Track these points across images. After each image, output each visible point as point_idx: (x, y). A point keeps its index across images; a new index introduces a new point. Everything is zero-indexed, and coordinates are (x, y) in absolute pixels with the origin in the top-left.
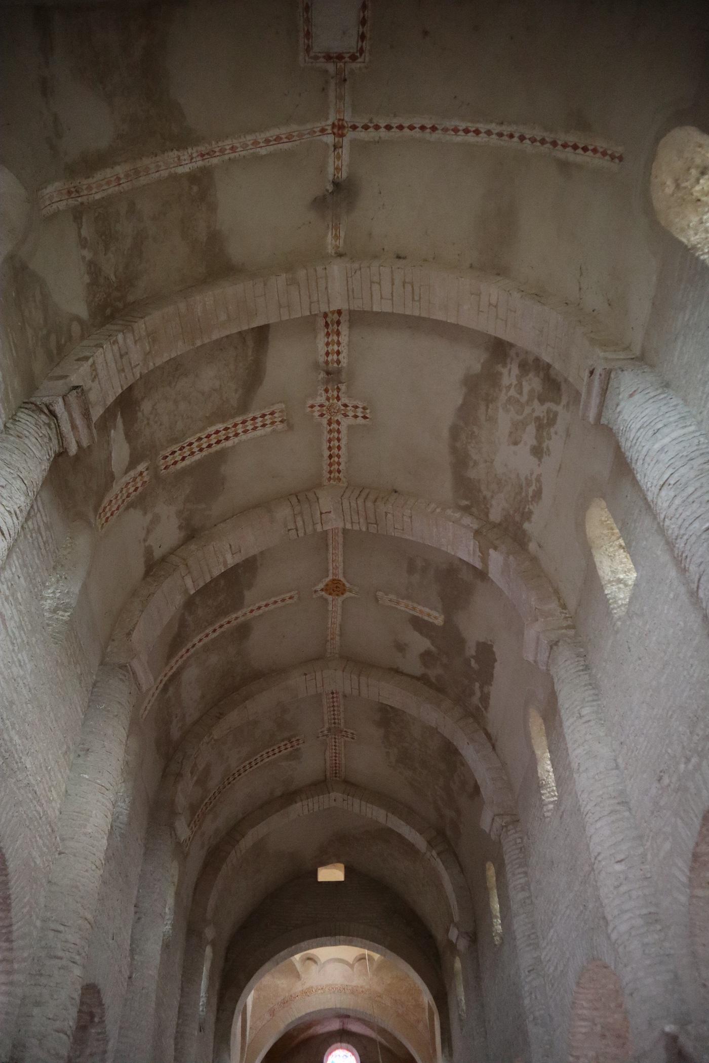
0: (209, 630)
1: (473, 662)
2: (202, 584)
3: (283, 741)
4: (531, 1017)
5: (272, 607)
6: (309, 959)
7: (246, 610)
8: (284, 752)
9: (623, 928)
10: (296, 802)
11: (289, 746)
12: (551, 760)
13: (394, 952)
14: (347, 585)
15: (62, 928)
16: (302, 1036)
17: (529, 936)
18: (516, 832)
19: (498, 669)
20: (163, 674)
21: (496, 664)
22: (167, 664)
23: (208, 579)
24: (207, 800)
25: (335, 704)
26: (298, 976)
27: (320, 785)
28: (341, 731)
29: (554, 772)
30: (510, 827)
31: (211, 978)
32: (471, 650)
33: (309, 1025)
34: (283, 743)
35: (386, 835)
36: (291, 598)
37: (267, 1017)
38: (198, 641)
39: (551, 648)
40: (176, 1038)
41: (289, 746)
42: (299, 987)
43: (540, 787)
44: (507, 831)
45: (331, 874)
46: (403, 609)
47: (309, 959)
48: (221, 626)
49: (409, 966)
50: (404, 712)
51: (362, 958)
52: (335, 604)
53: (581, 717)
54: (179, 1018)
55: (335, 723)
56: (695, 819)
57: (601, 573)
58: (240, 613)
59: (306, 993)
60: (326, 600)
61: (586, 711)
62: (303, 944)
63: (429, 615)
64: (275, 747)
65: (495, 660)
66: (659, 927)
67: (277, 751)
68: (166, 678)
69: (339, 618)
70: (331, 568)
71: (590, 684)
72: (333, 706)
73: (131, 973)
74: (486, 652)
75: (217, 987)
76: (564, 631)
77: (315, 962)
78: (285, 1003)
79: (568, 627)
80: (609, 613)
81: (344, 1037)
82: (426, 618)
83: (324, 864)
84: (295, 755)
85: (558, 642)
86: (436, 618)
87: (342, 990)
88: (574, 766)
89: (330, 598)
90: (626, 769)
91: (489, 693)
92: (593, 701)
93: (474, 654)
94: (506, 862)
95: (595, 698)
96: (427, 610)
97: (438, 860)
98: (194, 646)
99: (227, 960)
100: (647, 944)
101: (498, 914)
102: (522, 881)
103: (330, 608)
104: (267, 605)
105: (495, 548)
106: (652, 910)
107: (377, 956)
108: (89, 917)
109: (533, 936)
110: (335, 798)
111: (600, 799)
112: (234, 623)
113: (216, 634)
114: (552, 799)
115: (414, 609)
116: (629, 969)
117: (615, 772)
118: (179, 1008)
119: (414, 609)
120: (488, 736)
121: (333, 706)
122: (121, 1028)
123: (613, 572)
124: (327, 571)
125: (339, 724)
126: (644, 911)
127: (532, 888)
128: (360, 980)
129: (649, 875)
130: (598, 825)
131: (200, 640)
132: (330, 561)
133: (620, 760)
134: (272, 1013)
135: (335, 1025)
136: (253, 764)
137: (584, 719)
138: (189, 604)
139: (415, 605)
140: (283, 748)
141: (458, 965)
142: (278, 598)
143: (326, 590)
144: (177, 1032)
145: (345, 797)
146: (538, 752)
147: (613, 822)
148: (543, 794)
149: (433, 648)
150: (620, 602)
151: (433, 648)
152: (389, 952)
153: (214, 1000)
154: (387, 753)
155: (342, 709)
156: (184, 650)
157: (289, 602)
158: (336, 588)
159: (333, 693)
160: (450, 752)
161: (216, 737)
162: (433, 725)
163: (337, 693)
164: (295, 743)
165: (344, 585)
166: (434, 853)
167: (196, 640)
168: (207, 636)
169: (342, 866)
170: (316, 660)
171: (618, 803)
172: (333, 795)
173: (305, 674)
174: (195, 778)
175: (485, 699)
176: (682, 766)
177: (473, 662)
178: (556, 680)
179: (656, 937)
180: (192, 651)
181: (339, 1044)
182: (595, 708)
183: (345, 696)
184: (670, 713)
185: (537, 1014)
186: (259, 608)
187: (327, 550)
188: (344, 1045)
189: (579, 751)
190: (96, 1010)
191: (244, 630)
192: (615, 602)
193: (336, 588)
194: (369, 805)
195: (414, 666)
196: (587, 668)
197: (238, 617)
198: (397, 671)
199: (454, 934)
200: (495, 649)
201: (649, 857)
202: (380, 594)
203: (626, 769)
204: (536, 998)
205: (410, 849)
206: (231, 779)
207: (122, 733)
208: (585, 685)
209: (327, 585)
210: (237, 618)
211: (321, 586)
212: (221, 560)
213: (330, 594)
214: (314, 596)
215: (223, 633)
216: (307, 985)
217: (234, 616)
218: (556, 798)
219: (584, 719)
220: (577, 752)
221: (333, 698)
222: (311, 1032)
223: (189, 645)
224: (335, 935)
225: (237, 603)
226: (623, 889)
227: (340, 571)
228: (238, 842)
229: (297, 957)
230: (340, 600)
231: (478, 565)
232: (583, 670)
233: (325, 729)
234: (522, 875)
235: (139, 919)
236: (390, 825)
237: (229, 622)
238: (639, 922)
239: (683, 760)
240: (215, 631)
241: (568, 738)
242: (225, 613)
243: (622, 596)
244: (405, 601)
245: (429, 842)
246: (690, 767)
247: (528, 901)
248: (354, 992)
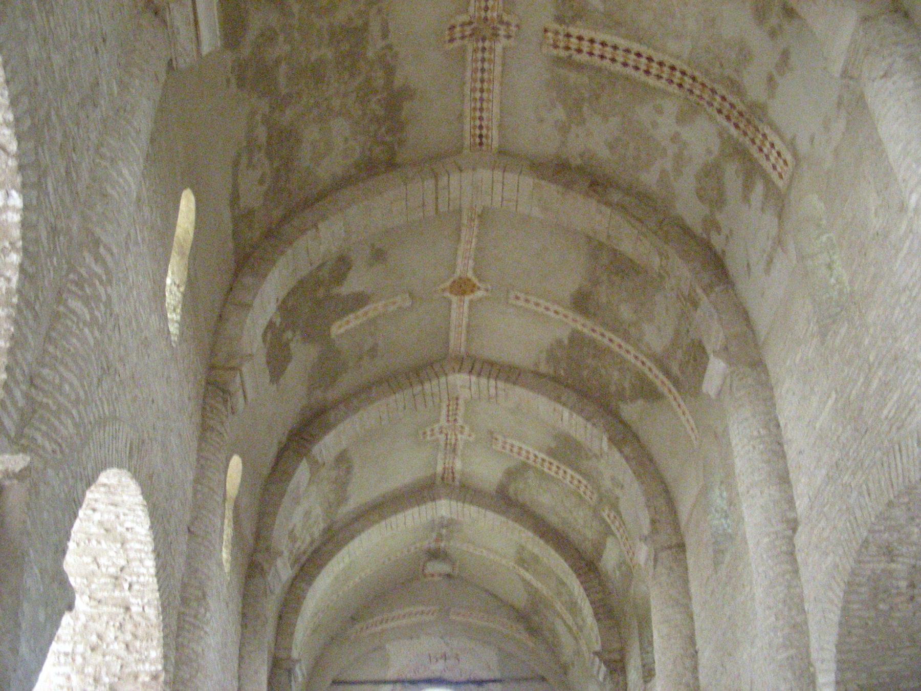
36: (517, 298)
52: (464, 268)
60: (475, 272)
69: (460, 253)
89: (470, 274)
121: (482, 91)
124: (470, 308)
125: (475, 51)
142: (531, 306)
143: (474, 285)
187: (468, 325)
209: (472, 291)
211: (479, 294)
213: (469, 280)
227: (454, 306)
230: (458, 273)
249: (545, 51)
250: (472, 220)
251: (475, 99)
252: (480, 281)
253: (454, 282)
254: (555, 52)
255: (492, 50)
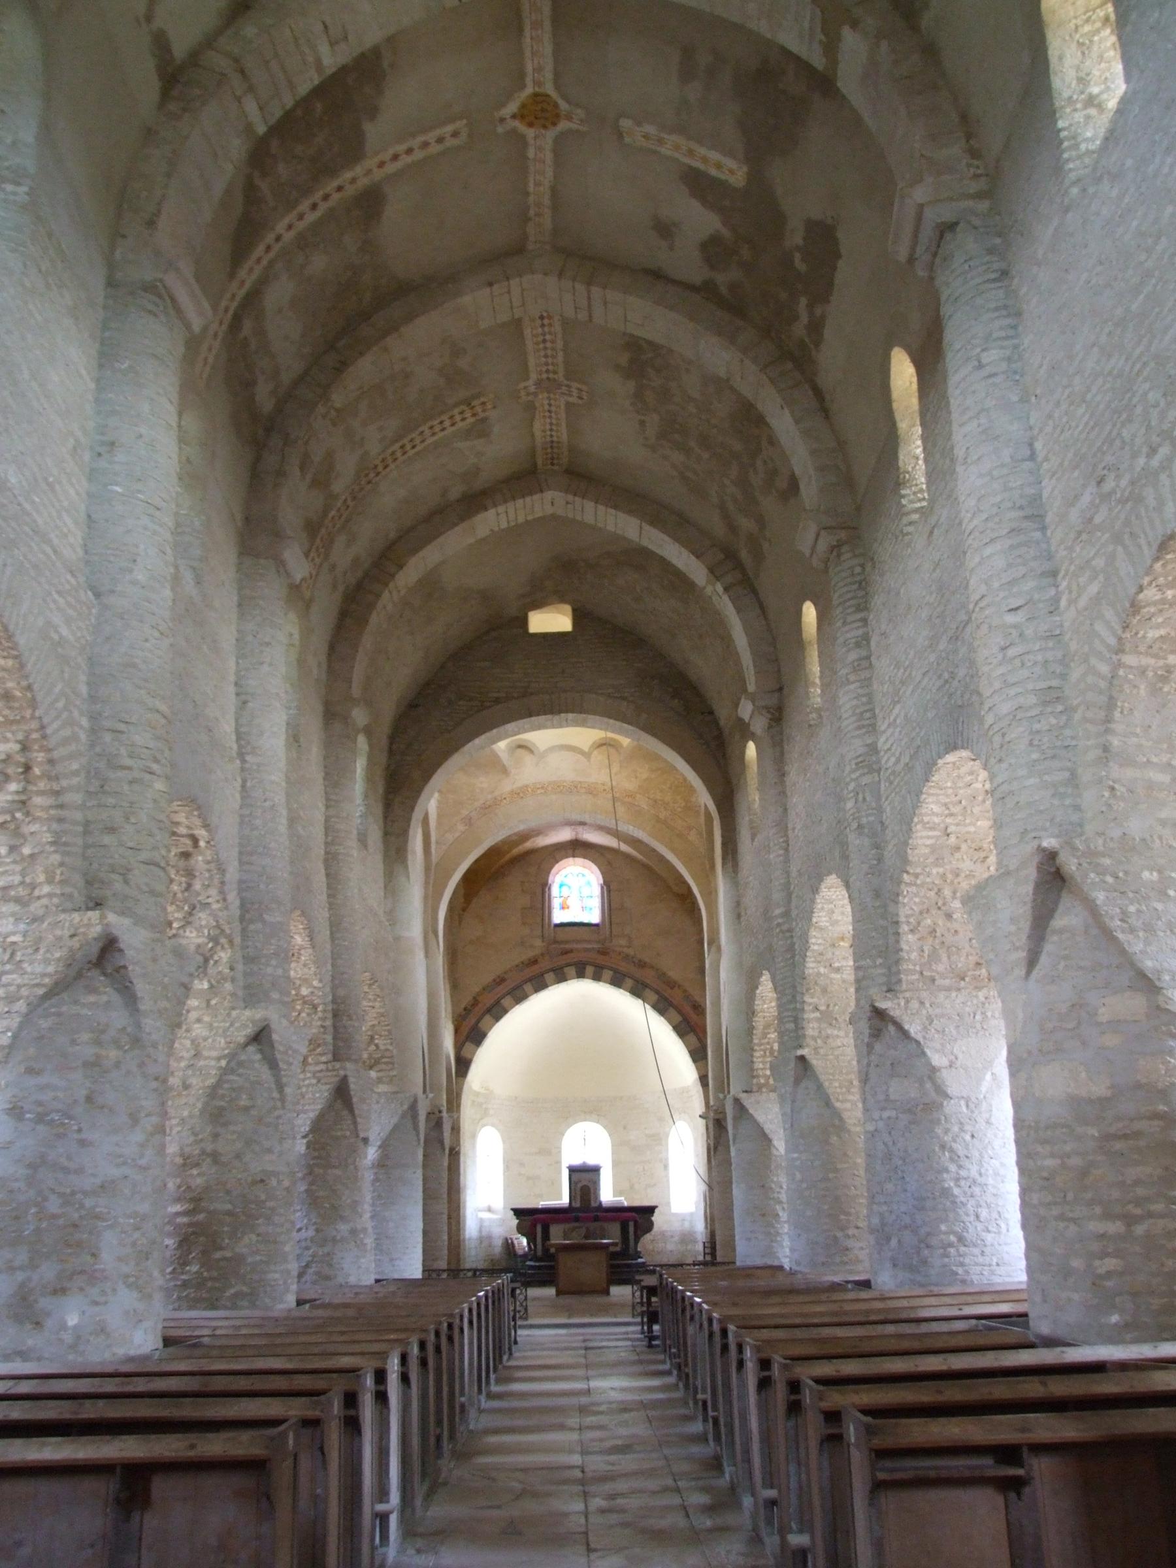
0: (304, 206)
1: (797, 257)
2: (278, 113)
3: (456, 405)
4: (855, 825)
5: (418, 155)
6: (520, 746)
7: (370, 163)
8: (461, 424)
9: (1005, 708)
10: (486, 509)
11: (468, 414)
12: (925, 439)
13: (654, 735)
14: (563, 105)
15: (122, 727)
16: (515, 851)
17: (862, 714)
18: (855, 556)
19: (844, 271)
20: (228, 295)
21: (841, 264)
22: (232, 275)
23: (289, 102)
24: (333, 513)
25: (548, 337)
26: (505, 771)
27: (524, 479)
28: (560, 386)
29: (926, 460)
30: (845, 548)
31: (369, 779)
32: (795, 237)
33: (525, 837)
34: (456, 411)
35: (640, 559)
36: (455, 134)
37: (461, 827)
38: (285, 228)
39: (941, 237)
40: (326, 861)
41: (468, 414)
42: (507, 786)
43: (899, 484)
44: (839, 556)
45: (553, 620)
46: (669, 153)
47: (520, 746)
48: (326, 197)
49: (674, 754)
50: (670, 351)
51: (601, 744)
52: (541, 143)
53: (980, 366)
54: (326, 835)
55: (547, 371)
56: (1146, 551)
57: (1056, 83)
58: (358, 170)
59: (520, 793)
60: (523, 138)
61: (992, 356)
62: (510, 727)
63: (719, 166)
64: (445, 417)
65: (839, 256)
66: (1060, 708)
67: (447, 423)
68: (235, 304)
69: (550, 173)
70: (529, 68)
71: (1005, 307)
72: (544, 341)
73: (244, 781)
74: (823, 238)
75: (381, 790)
76: (970, 203)
77: (531, 751)
78: (487, 809)
79: (979, 196)
80: (1058, 169)
81: (577, 848)
82: (713, 172)
83: (538, 604)
84: (480, 430)
85: (957, 224)
86: (731, 172)
87: (573, 789)
88: (959, 452)
89: (530, 133)
90: (1046, 459)
91: (823, 317)
92: (1007, 338)
93: (800, 242)
94: (835, 602)
95: (1011, 332)
96: (714, 156)
97: (725, 598)
98: (278, 238)
99: (391, 752)
100: (1038, 732)
101: (817, 681)
102: (860, 632)
103: (531, 153)
104: (409, 151)
105: (854, 24)
106: (1054, 683)
107: (625, 741)
108: (163, 708)
109: (868, 715)
110: (549, 502)
111: (995, 510)
112: (350, 191)
113: (318, 214)
114: (918, 505)
115: (691, 153)
116: (1004, 765)
117: (1028, 465)
118: (326, 821)
119: (691, 153)
120: (818, 393)
121: (544, 341)
122: (241, 853)
123: (1080, 80)
124: (522, 75)
125: (555, 372)
126: (1043, 685)
127: (873, 643)
128: (598, 773)
129: (1058, 632)
130: (988, 551)
131: (290, 227)
132: (528, 54)
133: (1038, 446)
134: (468, 821)
135: (565, 835)
136: (408, 447)
137: (988, 370)
138: (259, 156)
139: (693, 145)
140: (458, 418)
141: (751, 749)
144: (327, 853)
145: (570, 497)
146: (902, 425)
147: (1012, 547)
148: (903, 496)
149: (726, 232)
150: (1083, 147)
151: (726, 232)
152: (642, 733)
153: (379, 809)
154: (642, 423)
155: (560, 344)
156: (261, 248)
157: (450, 142)
158: (540, 112)
159: (542, 317)
160: (749, 419)
161: (338, 405)
162: (722, 373)
163: (550, 317)
164: (479, 409)
165: (556, 106)
166: (719, 588)
167: (281, 227)
168: (301, 217)
169: (568, 608)
170: (505, 257)
171: (1026, 517)
172: (549, 495)
173: (491, 284)
174: (309, 477)
175: (816, 327)
176: (1141, 461)
177: (797, 257)
178: (943, 298)
179: (1053, 721)
180: (277, 248)
181: (571, 860)
182: (1008, 353)
183: (565, 322)
184: (1138, 366)
185: (864, 821)
186: (395, 157)
187: (520, 30)
188: (579, 860)
189: (971, 427)
190: (201, 833)
191: (370, 203)
192: (1076, 146)
193: (540, 112)
194: (613, 511)
195: (686, 262)
196: (1005, 273)
197: (356, 177)
198: (657, 275)
199: (746, 710)
200: (840, 235)
201: (1063, 603)
202: (626, 123)
203: (1046, 459)
204: (864, 799)
205: (679, 582)
206: (372, 475)
207: (169, 410)
208: (997, 309)
209: (523, 106)
210: (353, 180)
211: (512, 107)
212: (311, 59)
213: (531, 125)
214: (500, 130)
215: (332, 210)
216: (519, 784)
217: (348, 175)
218: (925, 504)
219: (988, 370)
220: (967, 428)
221: (543, 325)
222: (529, 845)
223: (270, 238)
224: (560, 712)
225: (354, 150)
226: (1011, 652)
227: (549, 75)
228: (393, 576)
229: (502, 745)
230: (550, 134)
231: (818, 61)
232: (994, 280)
233: (530, 382)
234: (860, 624)
235: (245, 703)
236: (645, 543)
237: (340, 189)
238: (1032, 700)
239: (1145, 450)
240: (314, 207)
241: (954, 403)
242: (332, 172)
243: (1089, 134)
244: (674, 137)
245: (711, 570)
246: (1155, 462)
247: (865, 663)
248: (591, 791)
249: (492, 396)
250: (538, 215)
251: (550, 333)
252: (514, 131)
253: (554, 124)
254: (482, 399)
255: (540, 373)
